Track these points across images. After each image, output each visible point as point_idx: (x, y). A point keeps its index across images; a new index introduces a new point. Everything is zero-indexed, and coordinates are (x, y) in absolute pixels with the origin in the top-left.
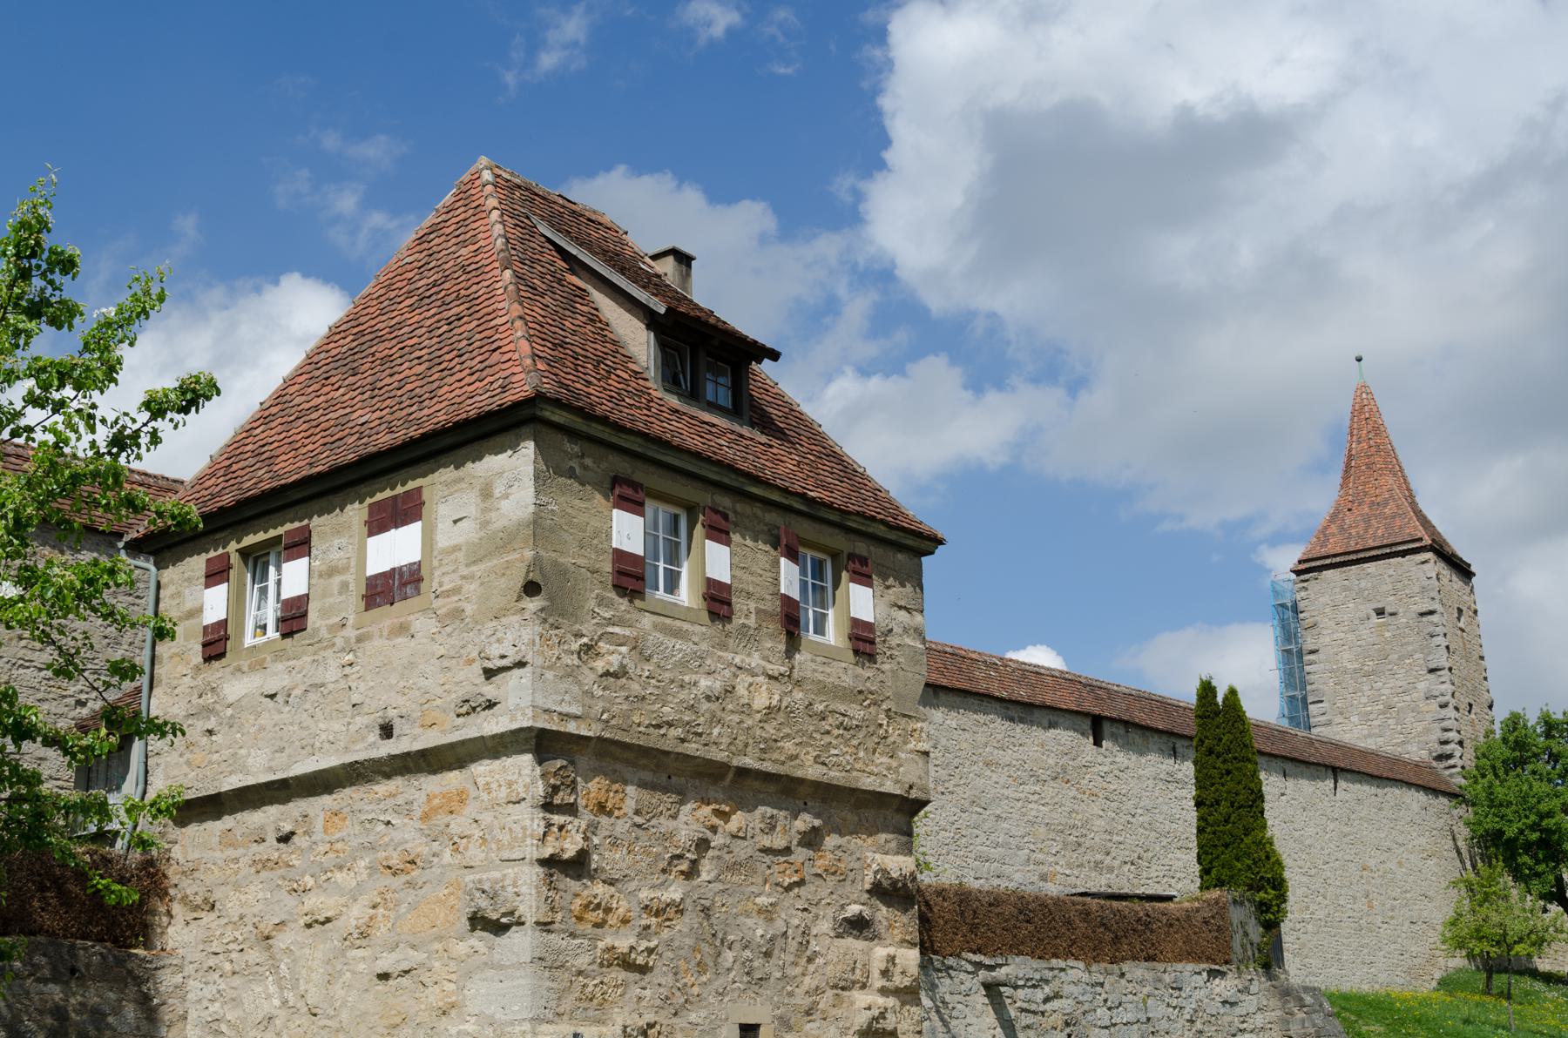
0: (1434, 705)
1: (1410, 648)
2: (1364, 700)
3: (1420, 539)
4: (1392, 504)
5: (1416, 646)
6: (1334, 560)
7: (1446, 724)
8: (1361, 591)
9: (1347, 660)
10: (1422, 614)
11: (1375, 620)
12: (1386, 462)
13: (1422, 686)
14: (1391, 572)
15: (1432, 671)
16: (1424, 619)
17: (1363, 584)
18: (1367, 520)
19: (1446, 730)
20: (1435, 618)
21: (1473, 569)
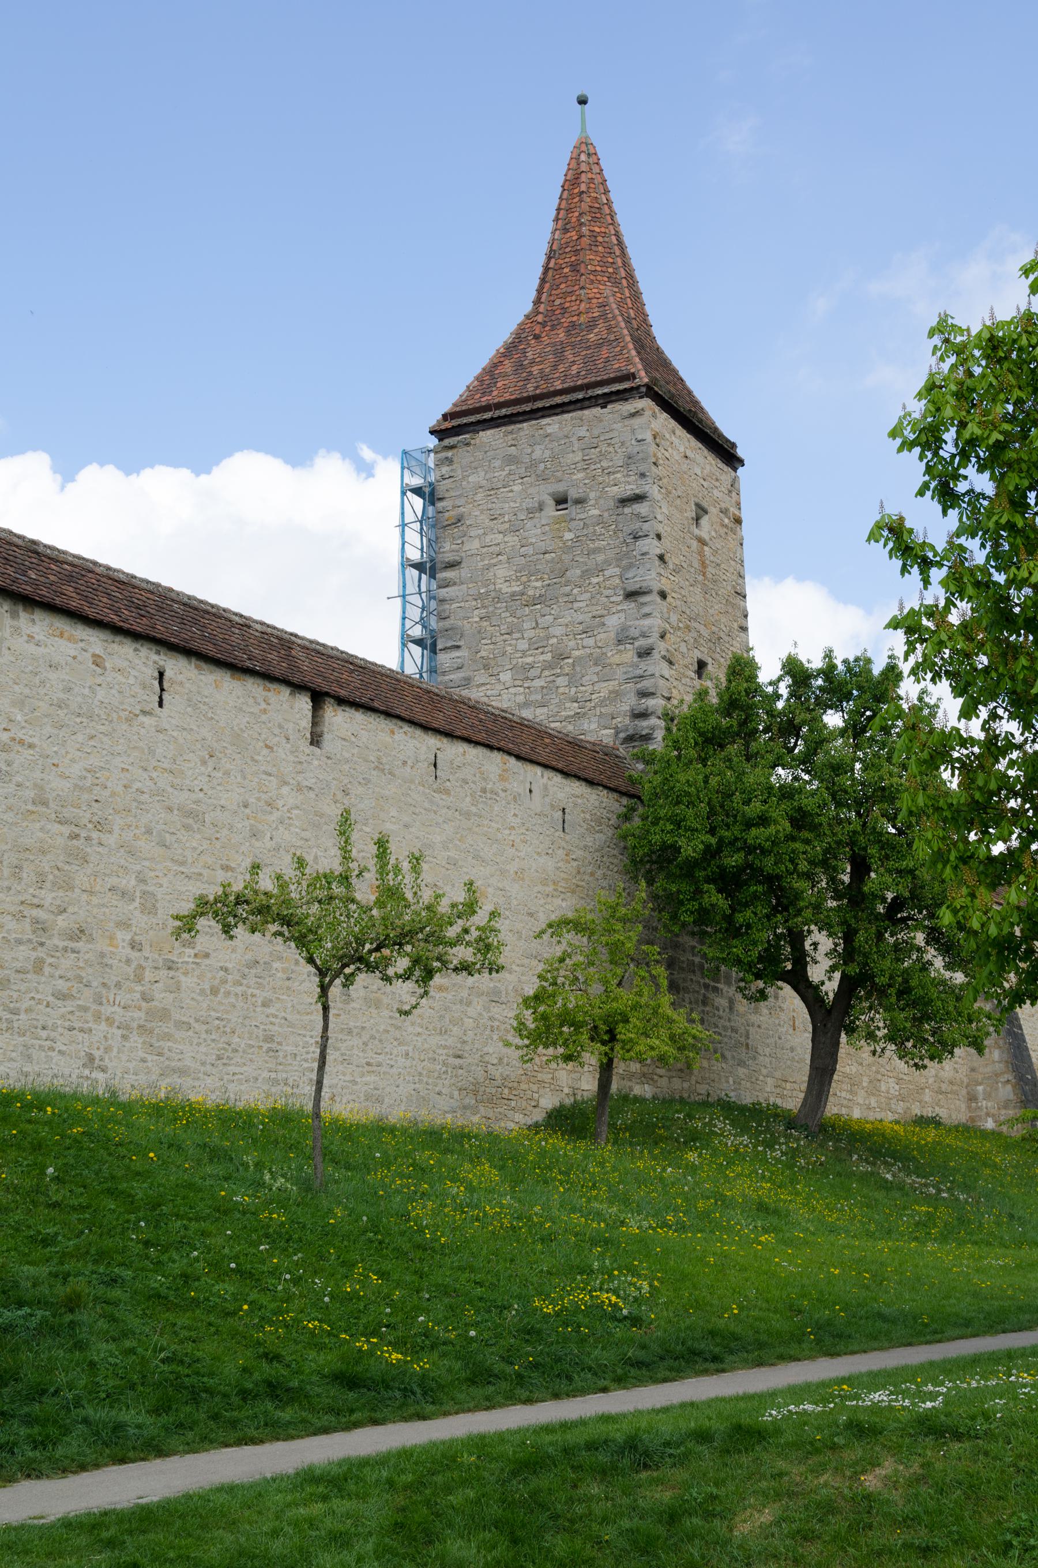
0: (629, 655)
1: (600, 558)
2: (523, 645)
3: (632, 376)
4: (601, 325)
5: (611, 554)
6: (498, 413)
7: (646, 684)
8: (533, 464)
9: (503, 578)
10: (625, 501)
11: (551, 511)
12: (603, 263)
13: (613, 621)
14: (582, 432)
16: (627, 510)
17: (538, 454)
18: (559, 355)
19: (644, 694)
20: (642, 508)
21: (740, 452)
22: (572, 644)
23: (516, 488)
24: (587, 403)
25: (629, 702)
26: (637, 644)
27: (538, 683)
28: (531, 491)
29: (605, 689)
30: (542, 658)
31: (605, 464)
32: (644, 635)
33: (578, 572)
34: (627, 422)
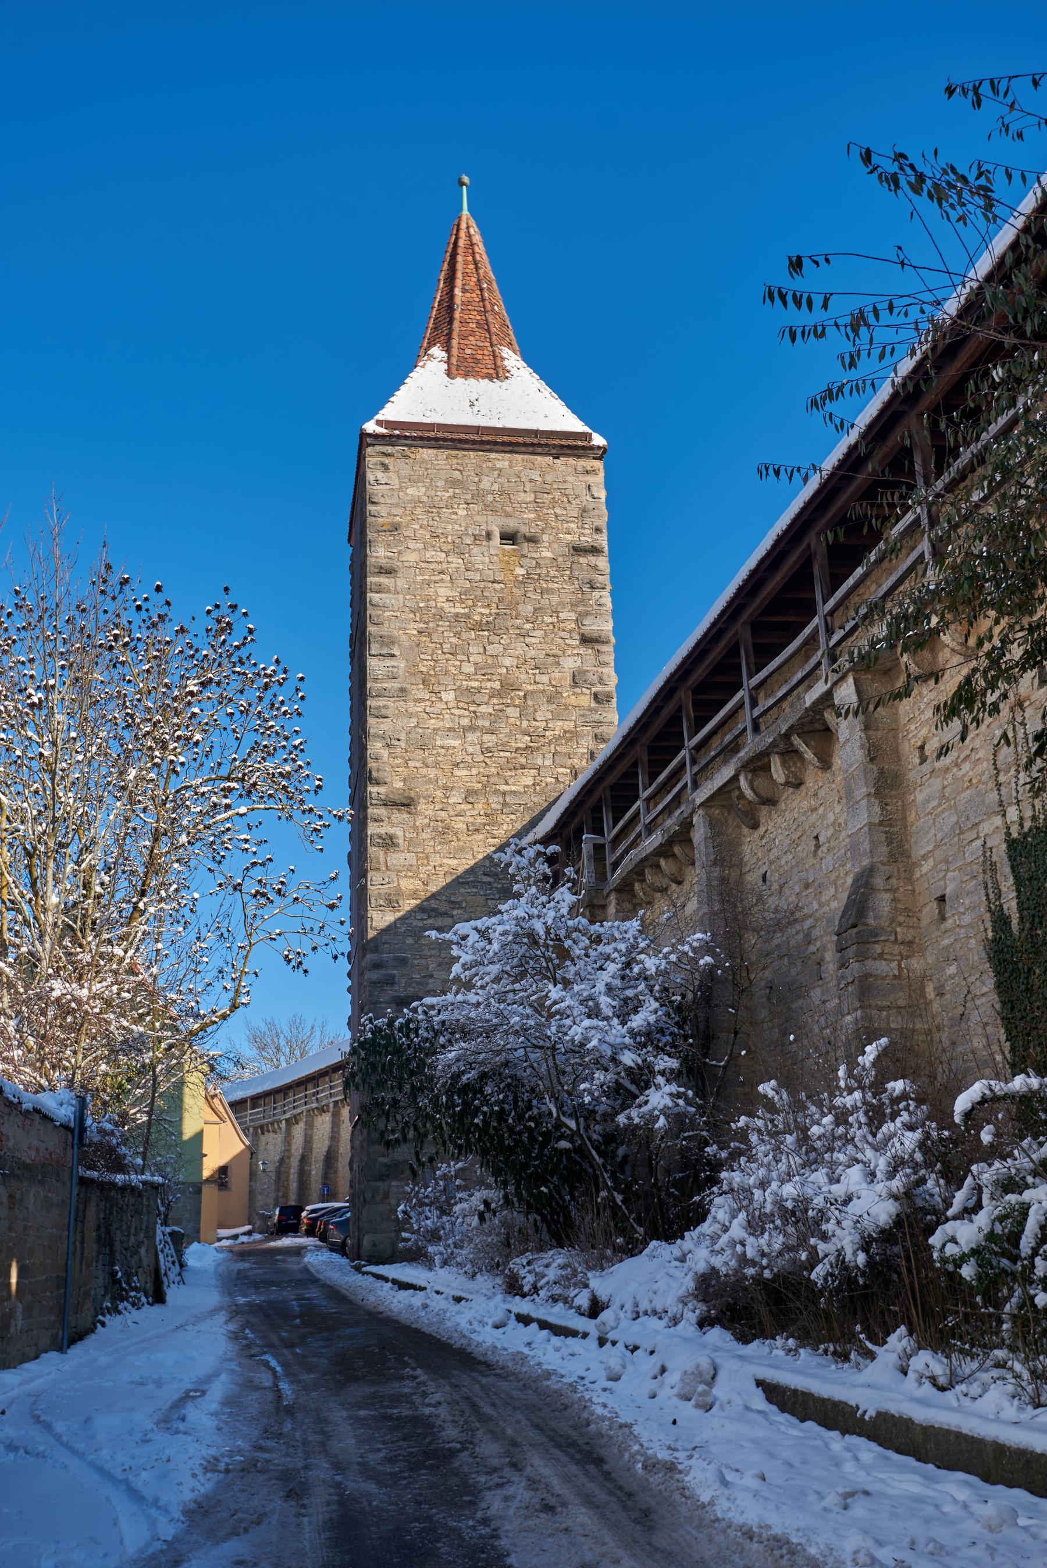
1: (555, 599)
2: (469, 668)
13: (570, 664)
16: (582, 560)
27: (483, 709)
28: (477, 518)
31: (559, 511)
34: (581, 477)
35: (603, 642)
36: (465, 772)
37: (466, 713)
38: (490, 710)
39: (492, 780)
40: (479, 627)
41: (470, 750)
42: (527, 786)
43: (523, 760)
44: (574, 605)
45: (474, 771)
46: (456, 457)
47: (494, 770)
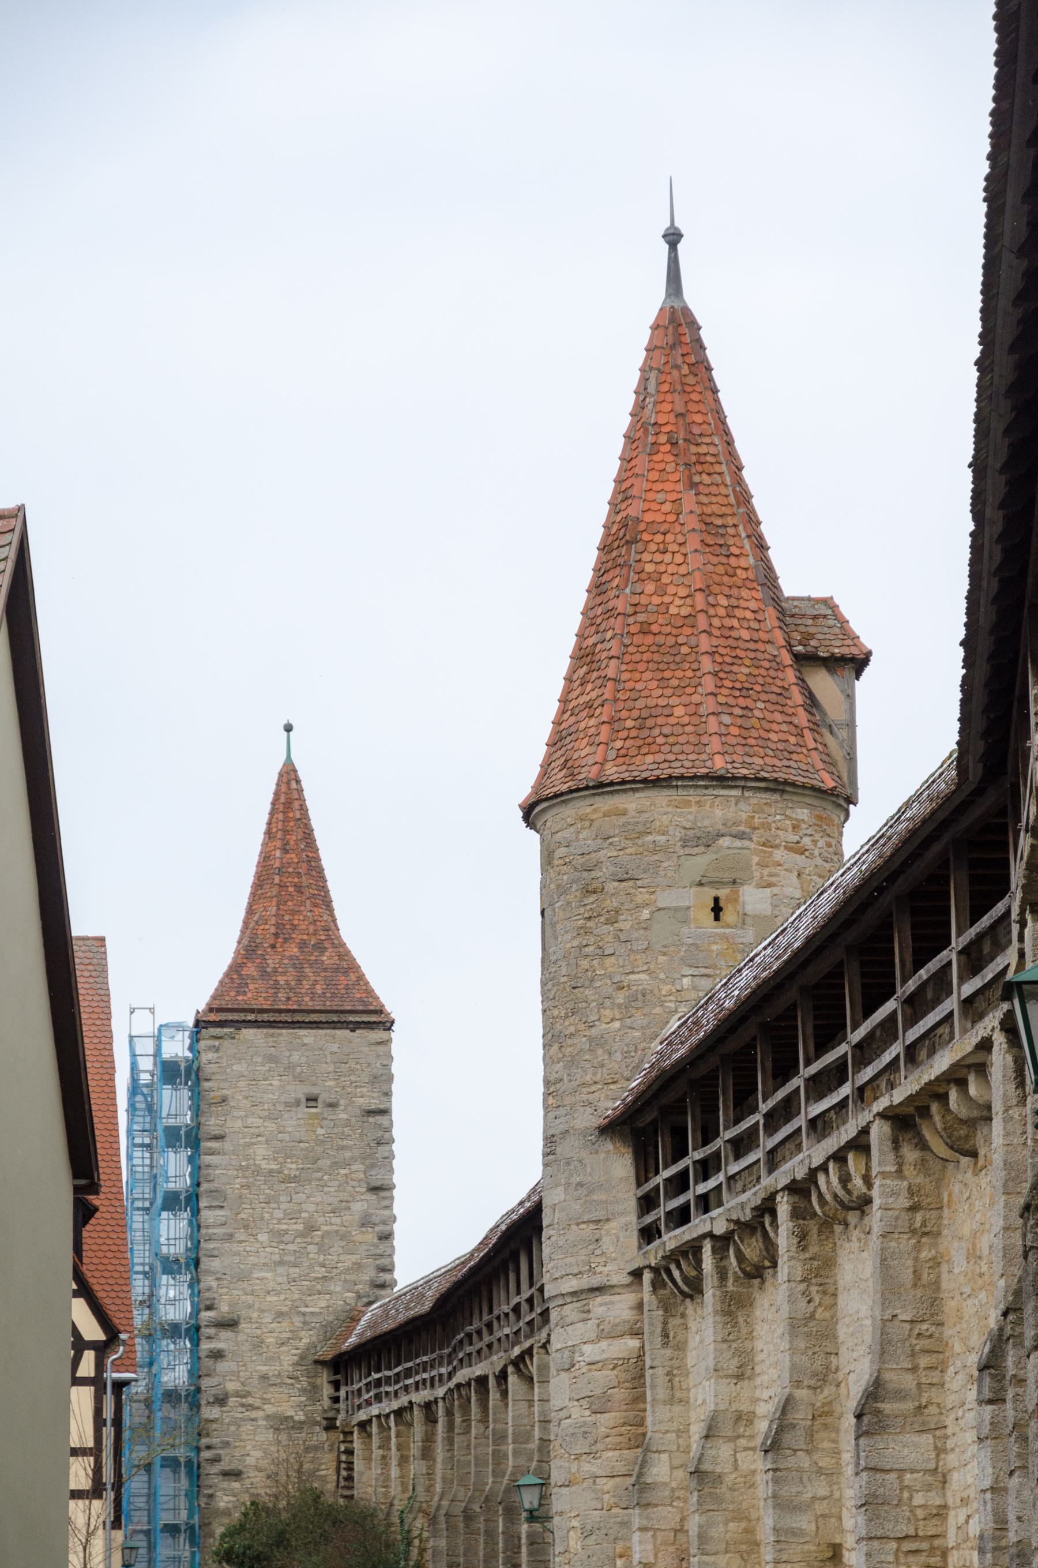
1: (348, 1154)
2: (279, 1214)
8: (290, 1067)
13: (358, 1207)
15: (375, 1189)
16: (371, 1120)
22: (321, 1220)
23: (276, 1083)
24: (339, 1025)
25: (369, 1274)
26: (377, 1229)
27: (292, 1247)
29: (349, 1260)
30: (295, 1227)
32: (384, 1223)
33: (328, 1162)
34: (373, 1048)
35: (385, 1189)
36: (276, 1298)
37: (277, 1250)
38: (295, 1248)
39: (296, 1304)
40: (290, 1179)
41: (280, 1280)
42: (322, 1308)
43: (319, 1287)
44: (363, 1158)
45: (282, 1297)
46: (272, 1036)
47: (297, 1296)
